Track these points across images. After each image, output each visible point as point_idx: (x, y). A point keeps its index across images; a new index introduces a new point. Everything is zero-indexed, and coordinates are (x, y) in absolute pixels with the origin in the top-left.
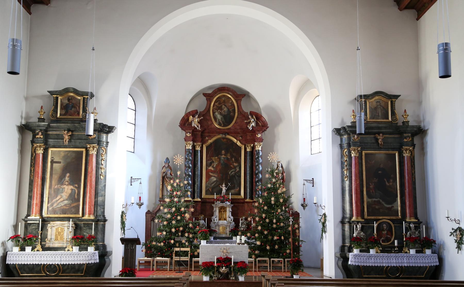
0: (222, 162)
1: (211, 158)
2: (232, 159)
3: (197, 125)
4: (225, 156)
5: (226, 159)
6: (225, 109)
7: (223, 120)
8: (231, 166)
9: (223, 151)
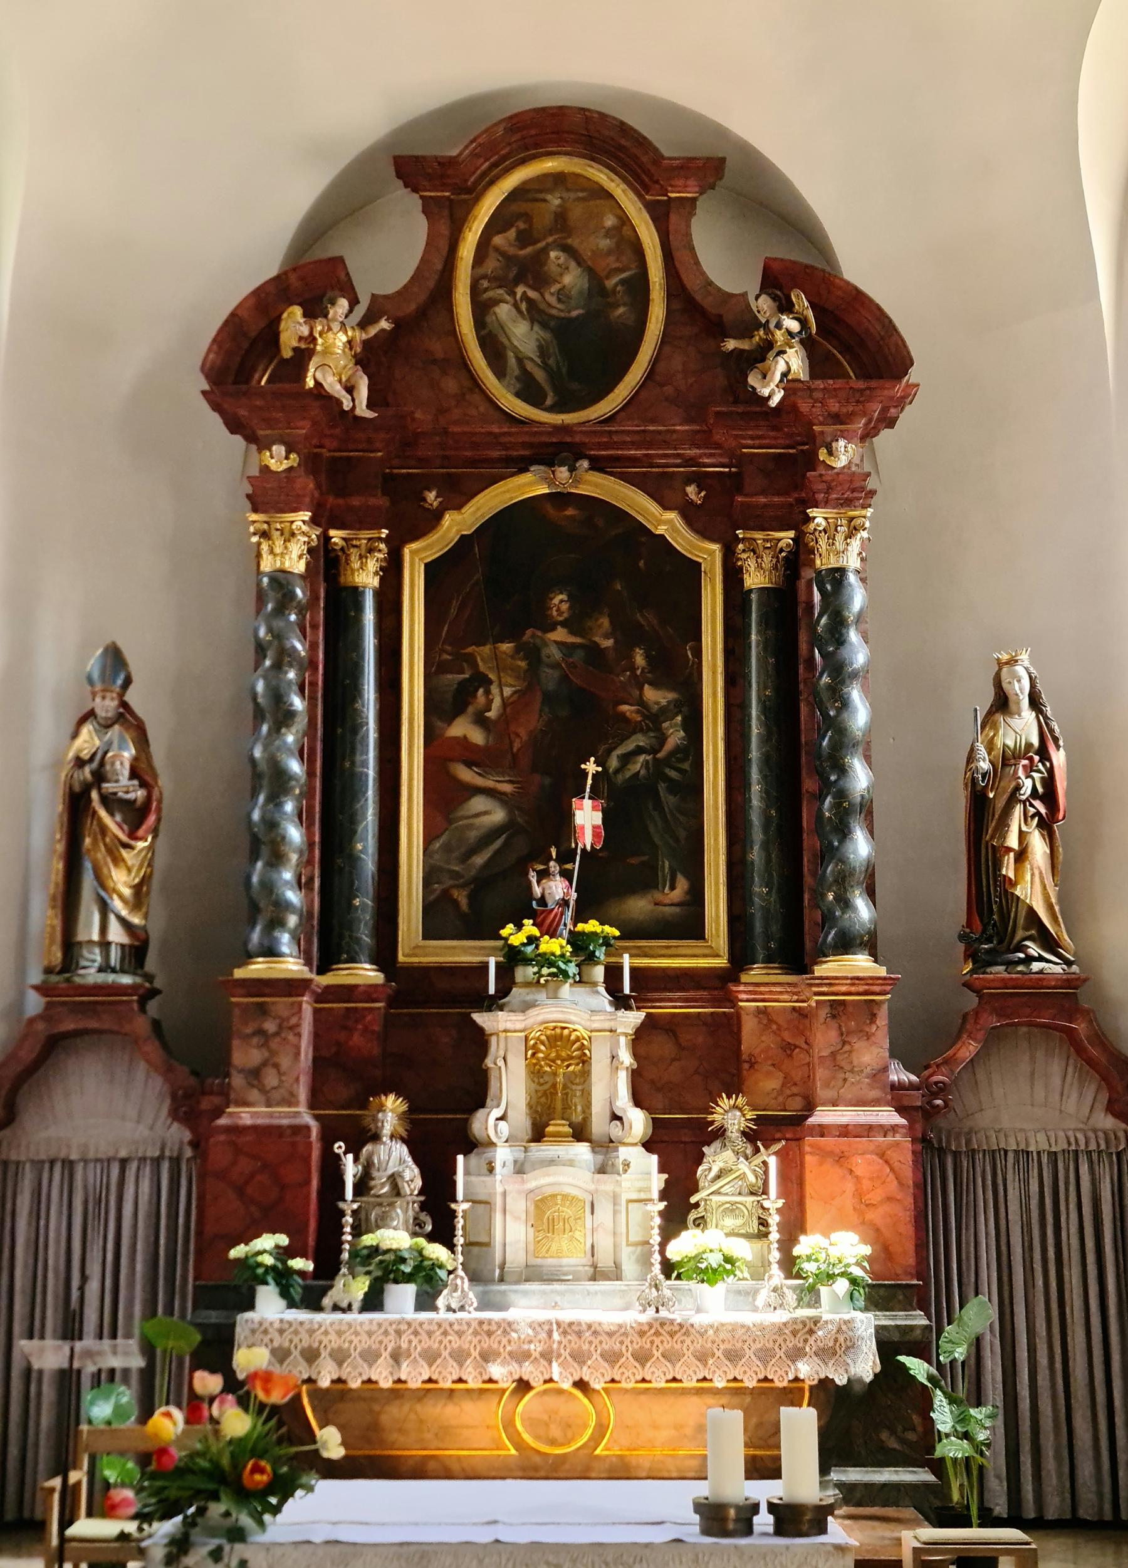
0: (550, 678)
1: (470, 650)
2: (630, 658)
3: (340, 381)
4: (572, 633)
5: (579, 655)
6: (567, 280)
7: (551, 362)
8: (625, 708)
9: (561, 597)
